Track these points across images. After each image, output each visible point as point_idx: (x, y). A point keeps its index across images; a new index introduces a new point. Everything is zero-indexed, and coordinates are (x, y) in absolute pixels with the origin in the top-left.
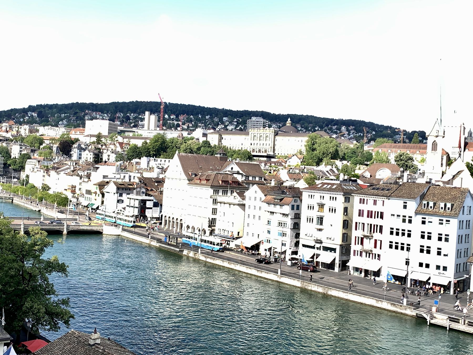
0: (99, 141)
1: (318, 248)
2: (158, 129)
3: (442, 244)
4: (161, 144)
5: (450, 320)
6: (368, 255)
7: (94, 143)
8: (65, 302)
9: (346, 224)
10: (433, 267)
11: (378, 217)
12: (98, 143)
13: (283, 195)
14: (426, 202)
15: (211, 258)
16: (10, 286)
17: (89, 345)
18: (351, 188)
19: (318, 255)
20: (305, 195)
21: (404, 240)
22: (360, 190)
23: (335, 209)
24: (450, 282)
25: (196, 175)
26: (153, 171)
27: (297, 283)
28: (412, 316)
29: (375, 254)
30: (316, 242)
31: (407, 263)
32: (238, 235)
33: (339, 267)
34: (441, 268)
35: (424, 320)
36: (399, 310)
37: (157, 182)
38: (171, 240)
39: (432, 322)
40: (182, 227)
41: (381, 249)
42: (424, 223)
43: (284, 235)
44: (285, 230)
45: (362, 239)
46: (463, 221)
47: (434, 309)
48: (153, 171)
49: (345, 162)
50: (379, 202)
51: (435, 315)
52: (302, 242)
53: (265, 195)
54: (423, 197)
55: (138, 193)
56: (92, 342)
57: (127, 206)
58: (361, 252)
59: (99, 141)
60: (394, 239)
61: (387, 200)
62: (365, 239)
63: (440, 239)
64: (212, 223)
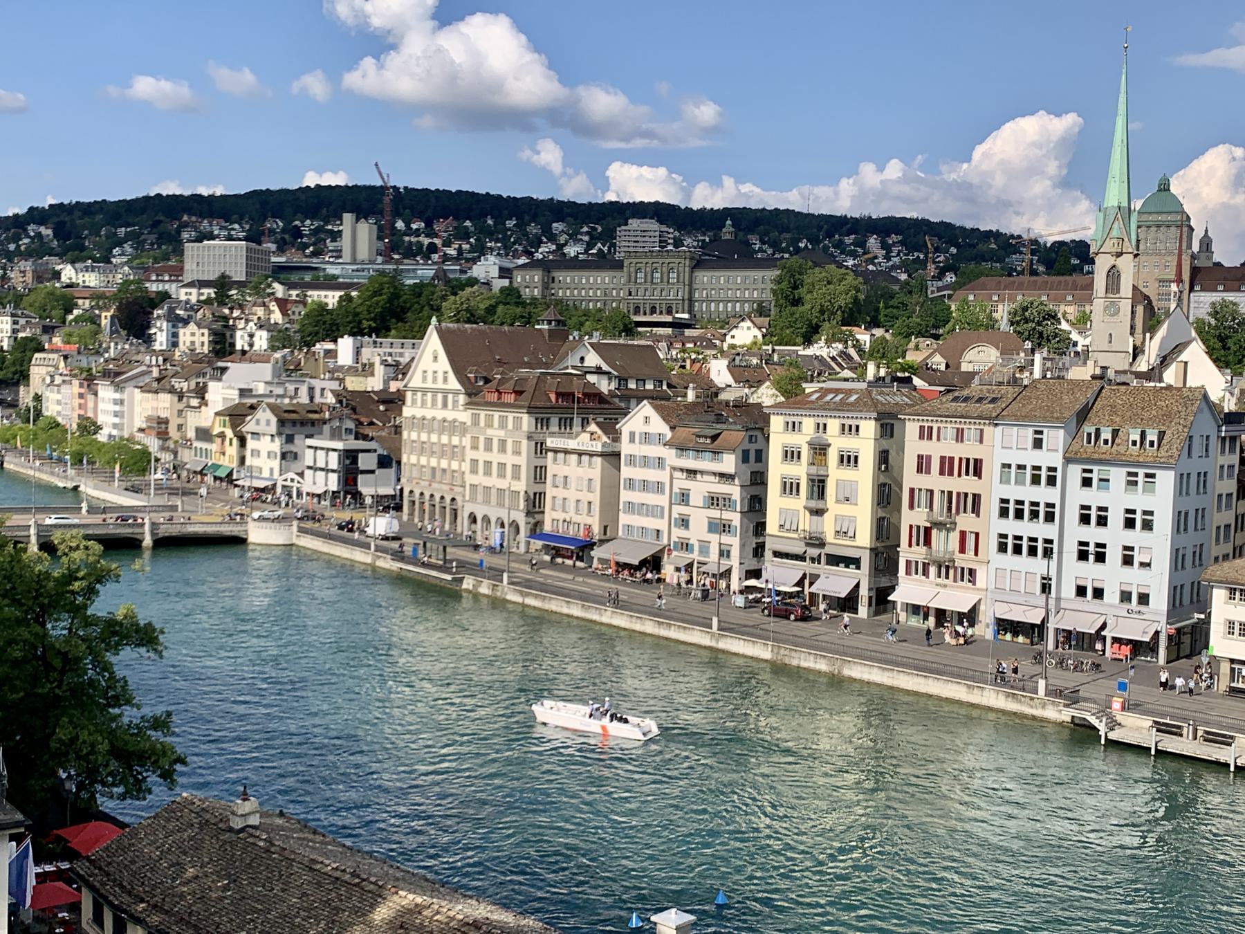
0: (222, 298)
1: (813, 560)
2: (380, 259)
3: (1136, 537)
4: (390, 301)
5: (1158, 730)
6: (943, 570)
7: (208, 302)
8: (160, 723)
9: (886, 496)
10: (1112, 596)
11: (967, 473)
12: (222, 303)
13: (718, 426)
14: (1092, 430)
15: (536, 596)
16: (14, 689)
17: (231, 830)
18: (898, 399)
19: (814, 578)
20: (776, 423)
21: (1041, 530)
22: (920, 406)
23: (856, 457)
24: (1157, 633)
25: (487, 381)
26: (372, 374)
27: (762, 651)
28: (1061, 724)
29: (963, 569)
30: (808, 545)
31: (1046, 588)
32: (605, 533)
33: (870, 605)
34: (1135, 598)
35: (1092, 732)
36: (1027, 710)
37: (384, 402)
38: (428, 553)
39: (1113, 736)
40: (456, 518)
41: (976, 554)
42: (1087, 482)
43: (725, 528)
44: (727, 515)
45: (928, 531)
46: (1189, 474)
47: (1117, 705)
48: (372, 374)
49: (879, 332)
50: (971, 431)
51: (1119, 718)
52: (770, 545)
53: (672, 428)
54: (1083, 415)
55: (335, 435)
56: (237, 824)
57: (309, 468)
58: (926, 567)
59: (222, 298)
60: (1012, 527)
61: (992, 428)
62: (934, 532)
63: (1130, 524)
64: (535, 504)
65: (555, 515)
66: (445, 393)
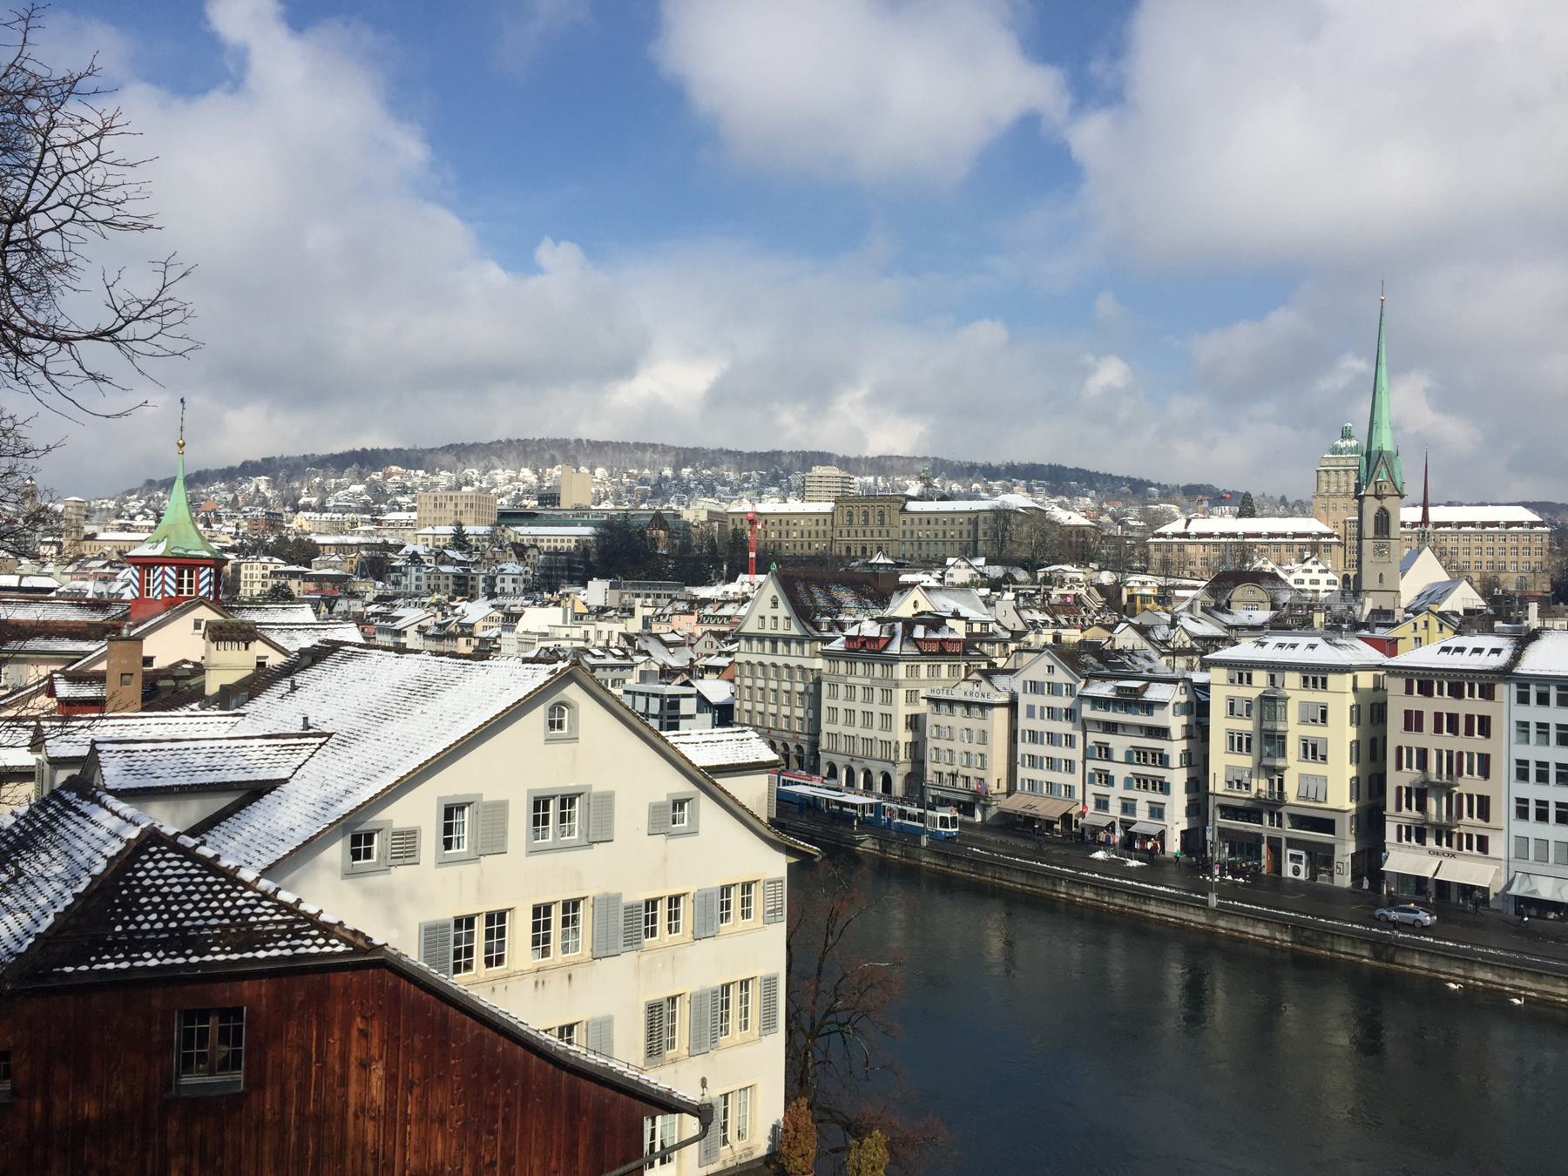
60: (1533, 791)
65: (938, 767)
66: (787, 640)
